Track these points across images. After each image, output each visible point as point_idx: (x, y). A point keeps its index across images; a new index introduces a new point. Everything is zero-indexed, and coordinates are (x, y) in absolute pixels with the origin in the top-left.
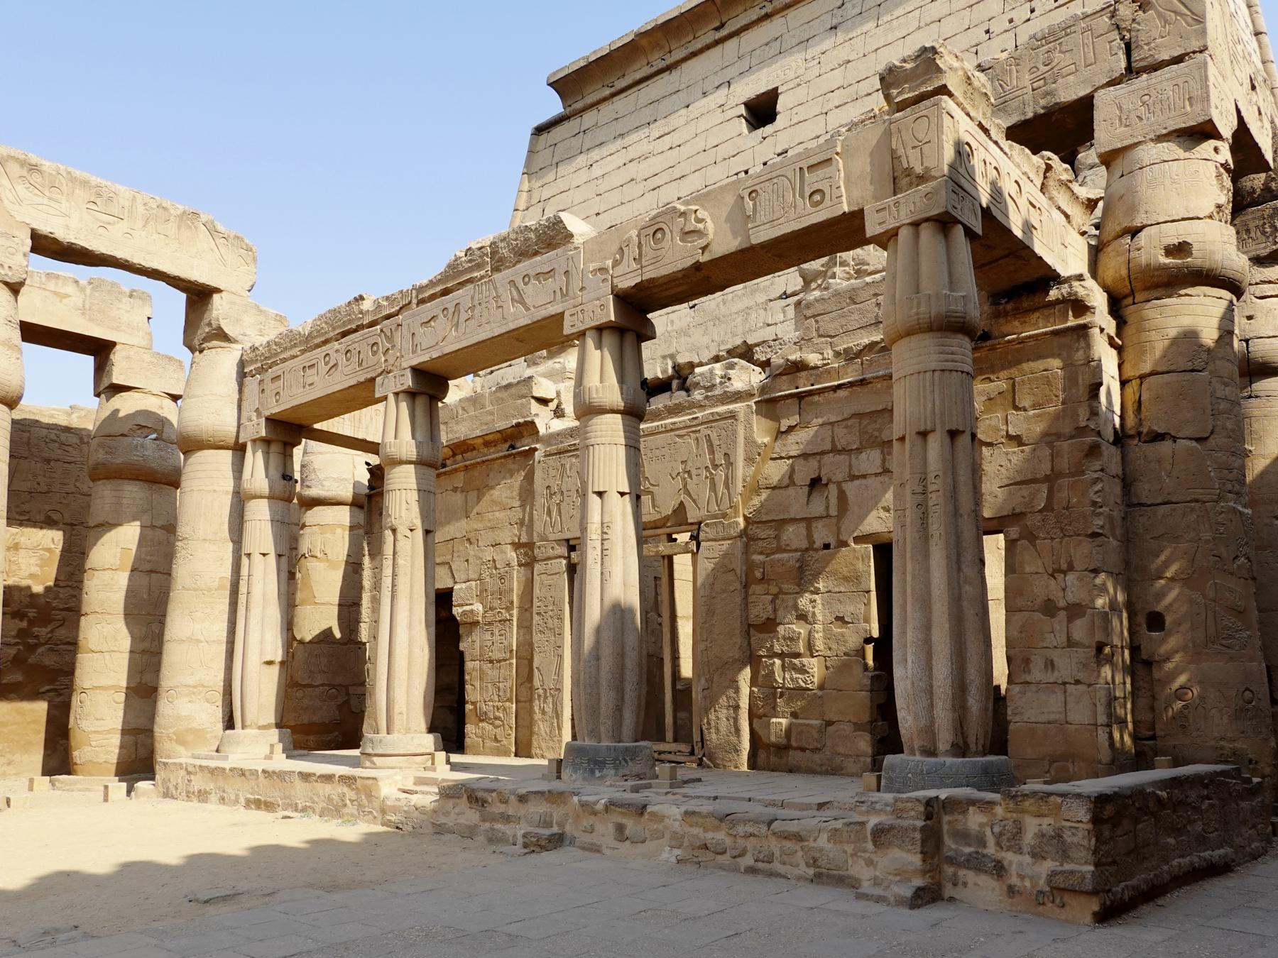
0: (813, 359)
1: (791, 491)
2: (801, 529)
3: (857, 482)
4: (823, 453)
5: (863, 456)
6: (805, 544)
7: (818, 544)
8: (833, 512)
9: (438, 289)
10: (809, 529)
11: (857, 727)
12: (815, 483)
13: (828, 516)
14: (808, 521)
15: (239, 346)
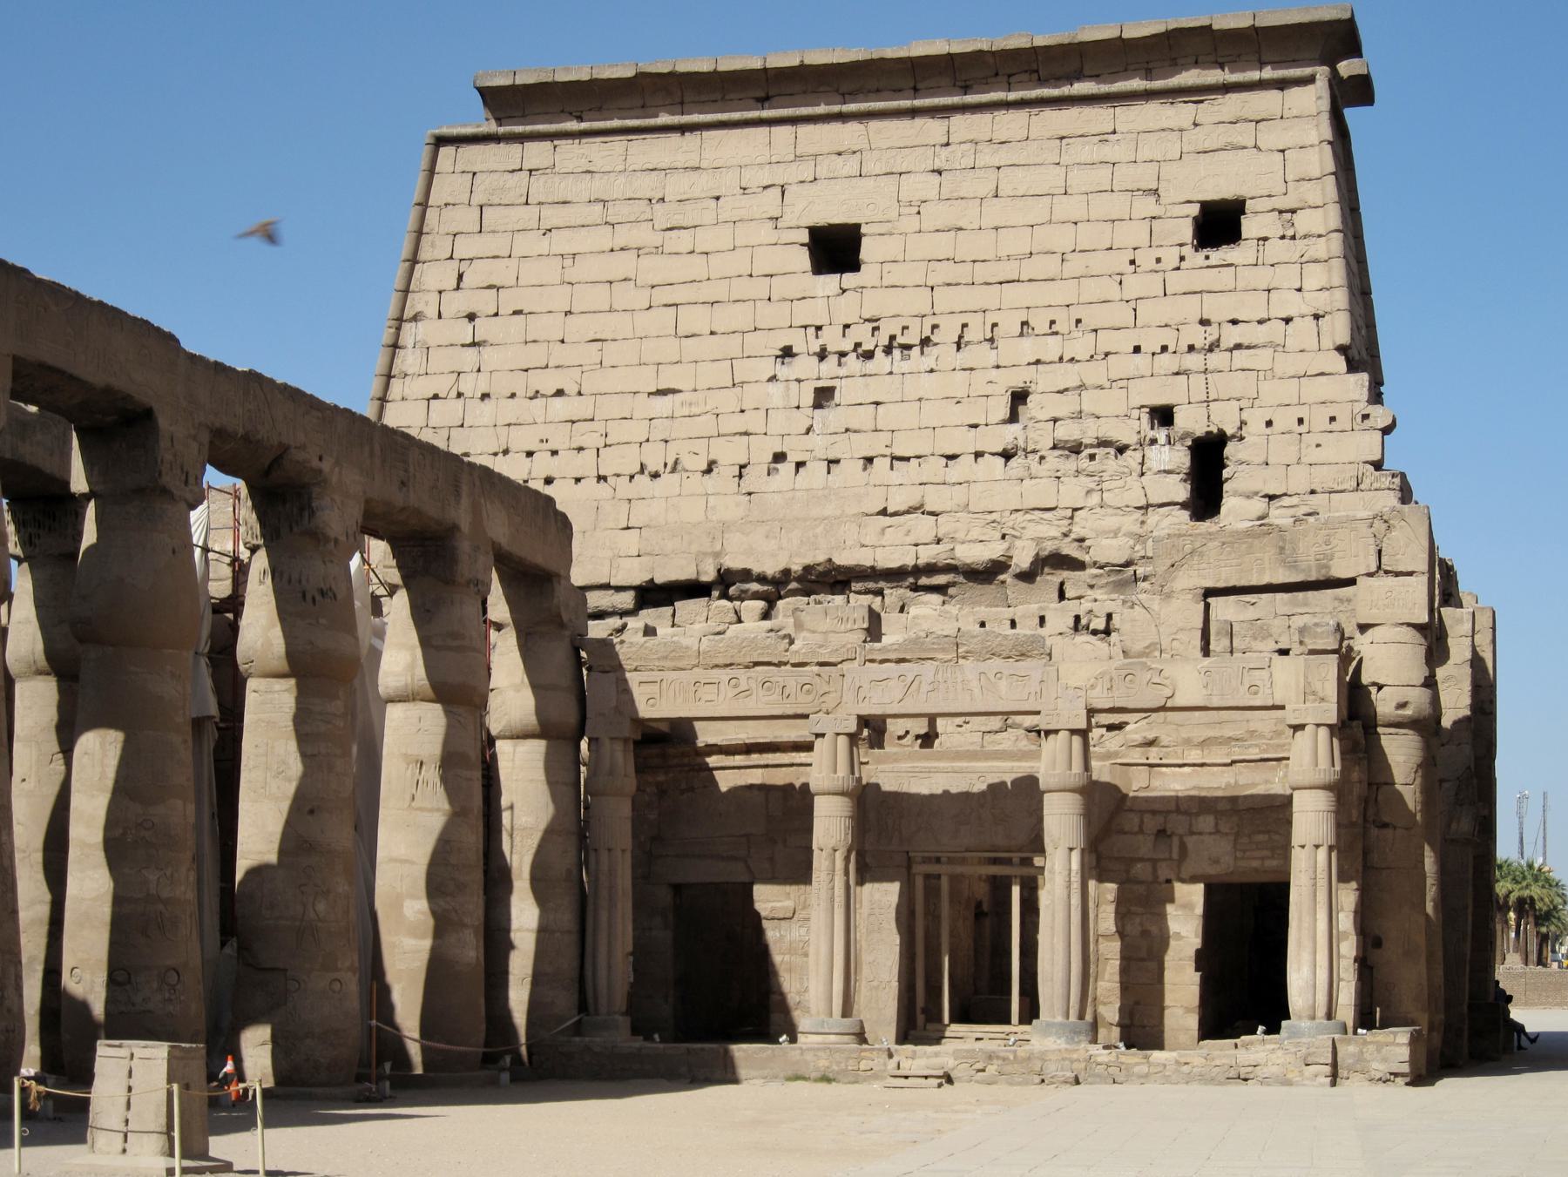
0: (1165, 740)
1: (1140, 837)
2: (1148, 866)
3: (1195, 837)
4: (1169, 812)
5: (1201, 819)
6: (1150, 878)
7: (1162, 878)
8: (1175, 856)
9: (893, 656)
10: (1155, 870)
11: (1188, 1010)
12: (1162, 833)
13: (1171, 859)
14: (1154, 862)
15: (567, 633)
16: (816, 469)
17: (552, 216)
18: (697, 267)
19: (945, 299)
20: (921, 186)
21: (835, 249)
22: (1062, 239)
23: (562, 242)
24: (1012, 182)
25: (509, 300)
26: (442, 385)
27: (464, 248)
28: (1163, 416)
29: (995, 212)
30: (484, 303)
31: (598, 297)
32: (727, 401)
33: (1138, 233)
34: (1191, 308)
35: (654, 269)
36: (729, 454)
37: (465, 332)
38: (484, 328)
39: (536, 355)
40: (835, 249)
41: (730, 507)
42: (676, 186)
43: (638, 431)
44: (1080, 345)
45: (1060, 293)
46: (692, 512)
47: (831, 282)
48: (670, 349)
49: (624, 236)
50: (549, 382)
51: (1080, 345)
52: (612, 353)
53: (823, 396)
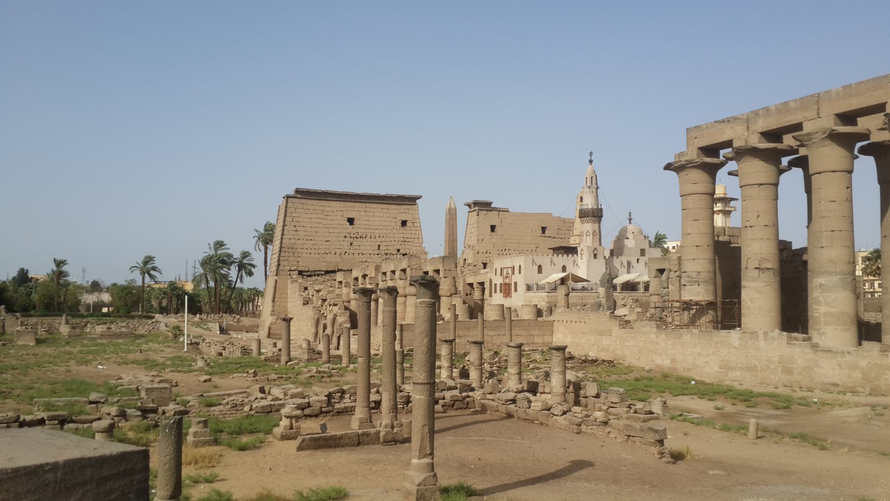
16: (351, 255)
17: (307, 211)
18: (331, 222)
19: (368, 231)
20: (362, 213)
21: (351, 221)
22: (384, 223)
23: (309, 216)
24: (376, 214)
25: (301, 224)
26: (292, 237)
27: (293, 215)
28: (398, 250)
29: (374, 219)
30: (297, 224)
31: (316, 225)
32: (337, 243)
33: (393, 224)
34: (402, 235)
35: (324, 222)
36: (338, 251)
37: (295, 229)
38: (297, 228)
39: (307, 233)
40: (351, 221)
41: (339, 259)
42: (326, 209)
43: (324, 247)
44: (387, 239)
45: (384, 231)
46: (333, 260)
47: (351, 227)
48: (327, 234)
49: (319, 216)
50: (309, 238)
51: (387, 239)
52: (319, 234)
53: (351, 244)
